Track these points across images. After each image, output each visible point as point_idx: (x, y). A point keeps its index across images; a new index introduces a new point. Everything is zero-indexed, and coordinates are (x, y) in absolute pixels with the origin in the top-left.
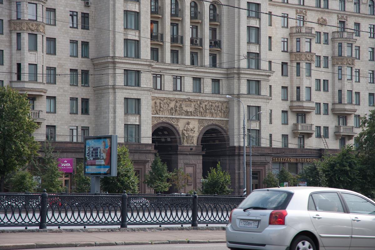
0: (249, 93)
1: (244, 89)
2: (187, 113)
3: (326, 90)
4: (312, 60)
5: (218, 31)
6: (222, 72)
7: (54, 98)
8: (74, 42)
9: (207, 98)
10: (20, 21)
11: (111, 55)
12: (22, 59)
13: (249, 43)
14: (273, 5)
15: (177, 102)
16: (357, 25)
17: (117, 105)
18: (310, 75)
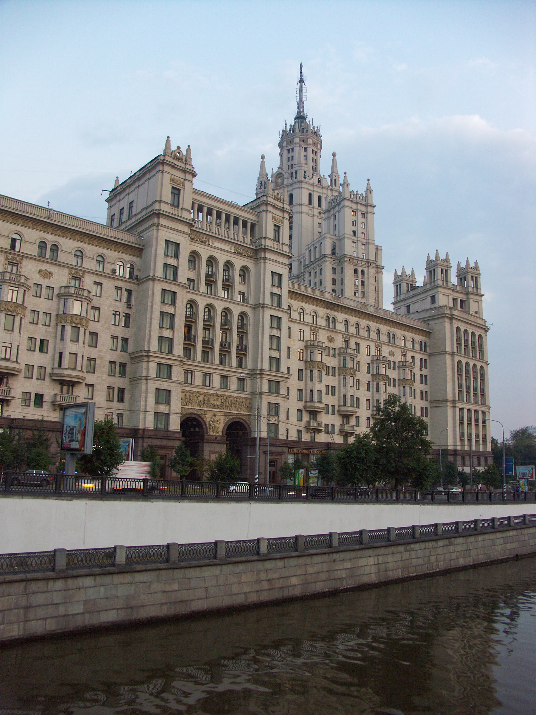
0: (270, 392)
1: (265, 388)
2: (214, 406)
3: (333, 394)
4: (323, 368)
5: (244, 338)
6: (247, 372)
7: (92, 386)
8: (114, 337)
9: (232, 394)
10: (66, 315)
11: (146, 349)
12: (64, 348)
13: (271, 349)
14: (292, 321)
15: (205, 396)
16: (357, 344)
17: (149, 395)
18: (321, 381)
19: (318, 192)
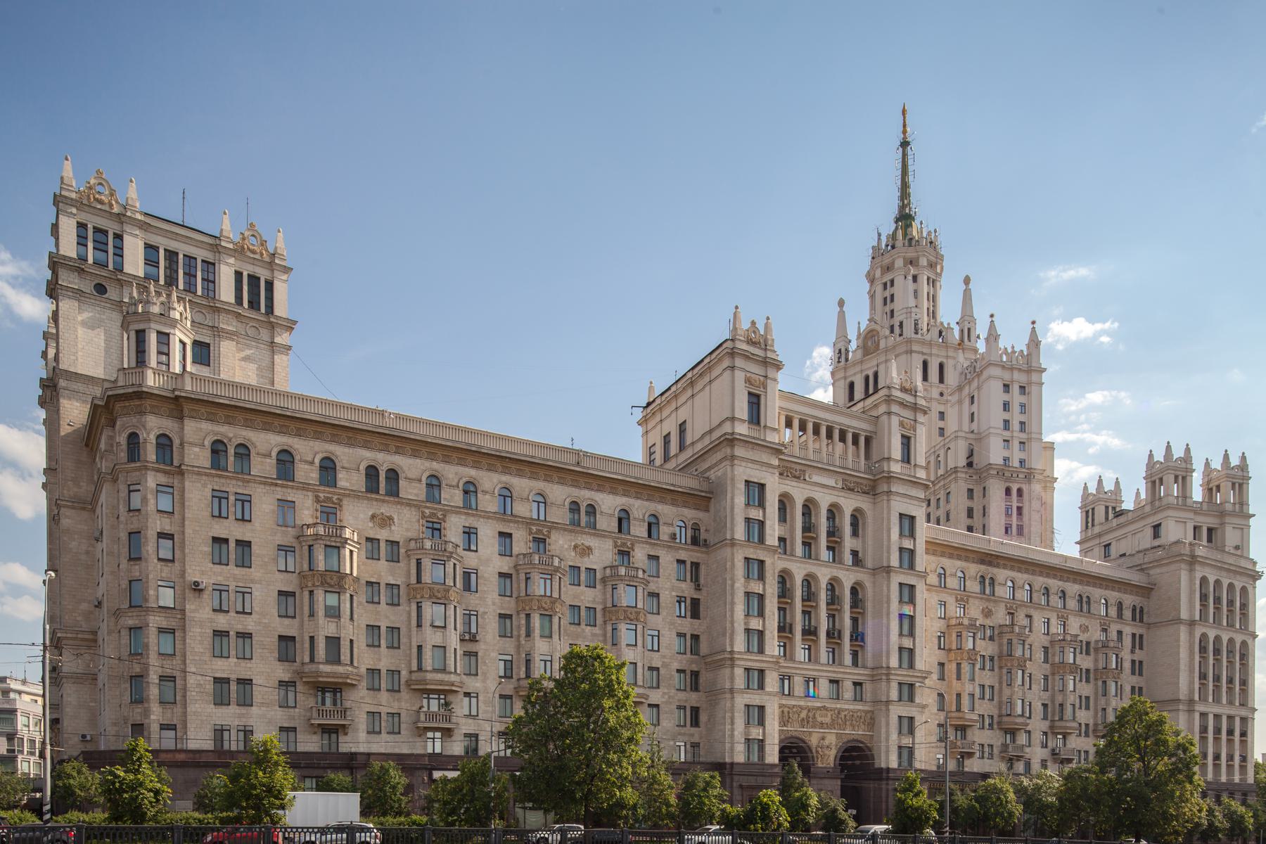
0: (900, 700)
1: (894, 695)
2: (822, 725)
4: (976, 659)
5: (860, 621)
6: (866, 672)
7: (657, 706)
8: (680, 635)
9: (846, 707)
11: (729, 649)
13: (901, 635)
15: (809, 711)
17: (736, 714)
18: (973, 680)
19: (938, 356)
